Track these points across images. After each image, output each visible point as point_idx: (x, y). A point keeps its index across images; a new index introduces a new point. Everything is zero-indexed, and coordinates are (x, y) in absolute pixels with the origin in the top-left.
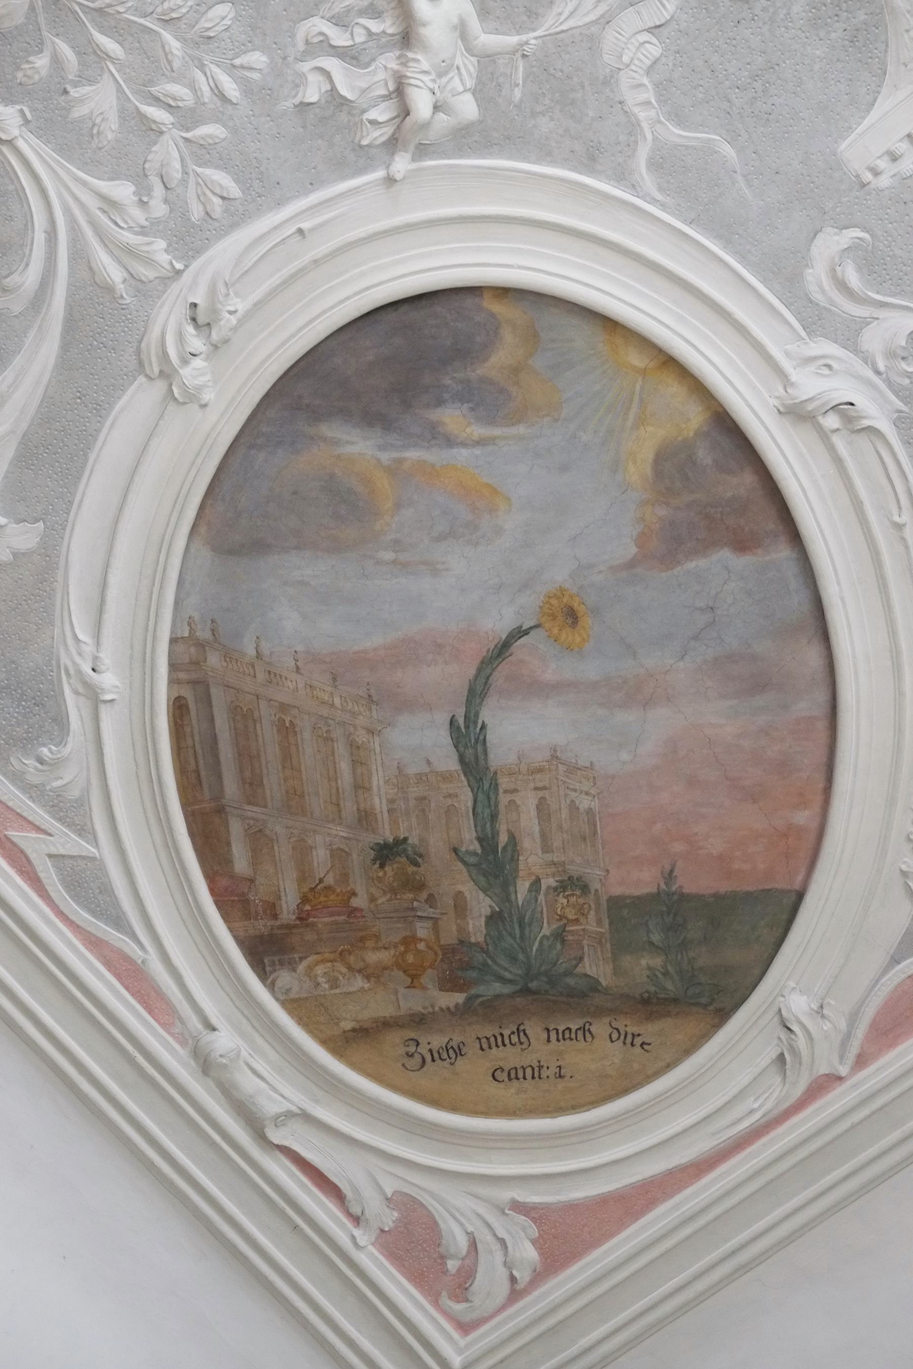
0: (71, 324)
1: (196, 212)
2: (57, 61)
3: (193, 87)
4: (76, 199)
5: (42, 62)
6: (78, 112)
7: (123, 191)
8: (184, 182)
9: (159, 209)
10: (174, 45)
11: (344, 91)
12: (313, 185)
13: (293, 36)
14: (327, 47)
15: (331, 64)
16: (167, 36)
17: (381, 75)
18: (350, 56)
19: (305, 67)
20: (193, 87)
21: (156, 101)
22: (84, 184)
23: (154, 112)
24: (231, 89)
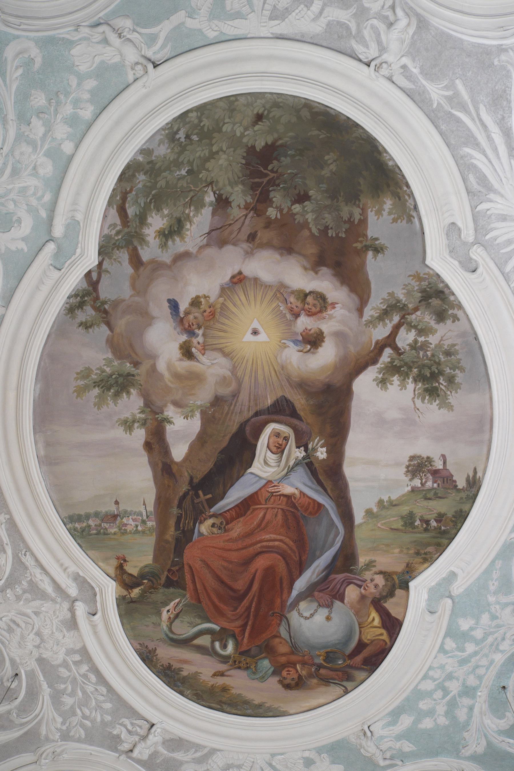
0: (26, 733)
1: (72, 734)
2: (66, 688)
3: (91, 713)
4: (48, 713)
5: (63, 686)
6: (62, 699)
7: (59, 720)
8: (74, 727)
9: (64, 728)
10: (94, 703)
11: (122, 737)
12: (102, 746)
13: (120, 719)
14: (125, 726)
15: (124, 730)
16: (94, 701)
17: (133, 739)
18: (130, 732)
19: (118, 726)
20: (91, 713)
21: (81, 710)
22: (52, 712)
23: (78, 711)
24: (99, 719)
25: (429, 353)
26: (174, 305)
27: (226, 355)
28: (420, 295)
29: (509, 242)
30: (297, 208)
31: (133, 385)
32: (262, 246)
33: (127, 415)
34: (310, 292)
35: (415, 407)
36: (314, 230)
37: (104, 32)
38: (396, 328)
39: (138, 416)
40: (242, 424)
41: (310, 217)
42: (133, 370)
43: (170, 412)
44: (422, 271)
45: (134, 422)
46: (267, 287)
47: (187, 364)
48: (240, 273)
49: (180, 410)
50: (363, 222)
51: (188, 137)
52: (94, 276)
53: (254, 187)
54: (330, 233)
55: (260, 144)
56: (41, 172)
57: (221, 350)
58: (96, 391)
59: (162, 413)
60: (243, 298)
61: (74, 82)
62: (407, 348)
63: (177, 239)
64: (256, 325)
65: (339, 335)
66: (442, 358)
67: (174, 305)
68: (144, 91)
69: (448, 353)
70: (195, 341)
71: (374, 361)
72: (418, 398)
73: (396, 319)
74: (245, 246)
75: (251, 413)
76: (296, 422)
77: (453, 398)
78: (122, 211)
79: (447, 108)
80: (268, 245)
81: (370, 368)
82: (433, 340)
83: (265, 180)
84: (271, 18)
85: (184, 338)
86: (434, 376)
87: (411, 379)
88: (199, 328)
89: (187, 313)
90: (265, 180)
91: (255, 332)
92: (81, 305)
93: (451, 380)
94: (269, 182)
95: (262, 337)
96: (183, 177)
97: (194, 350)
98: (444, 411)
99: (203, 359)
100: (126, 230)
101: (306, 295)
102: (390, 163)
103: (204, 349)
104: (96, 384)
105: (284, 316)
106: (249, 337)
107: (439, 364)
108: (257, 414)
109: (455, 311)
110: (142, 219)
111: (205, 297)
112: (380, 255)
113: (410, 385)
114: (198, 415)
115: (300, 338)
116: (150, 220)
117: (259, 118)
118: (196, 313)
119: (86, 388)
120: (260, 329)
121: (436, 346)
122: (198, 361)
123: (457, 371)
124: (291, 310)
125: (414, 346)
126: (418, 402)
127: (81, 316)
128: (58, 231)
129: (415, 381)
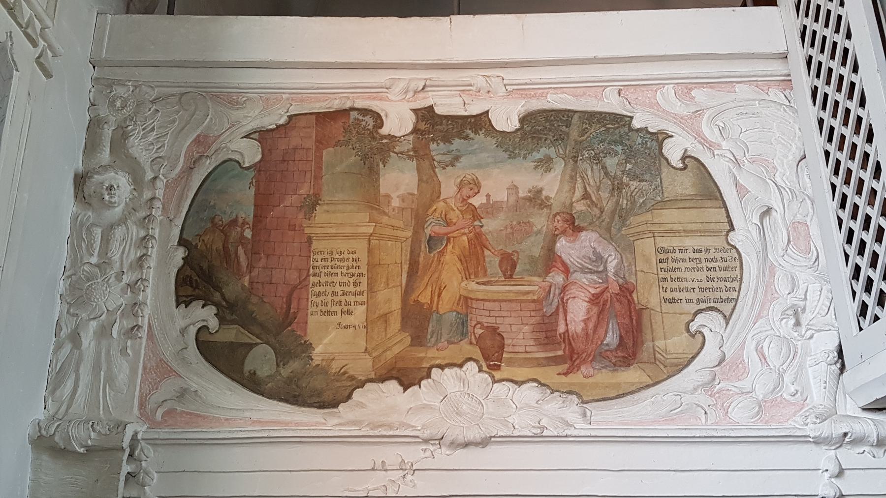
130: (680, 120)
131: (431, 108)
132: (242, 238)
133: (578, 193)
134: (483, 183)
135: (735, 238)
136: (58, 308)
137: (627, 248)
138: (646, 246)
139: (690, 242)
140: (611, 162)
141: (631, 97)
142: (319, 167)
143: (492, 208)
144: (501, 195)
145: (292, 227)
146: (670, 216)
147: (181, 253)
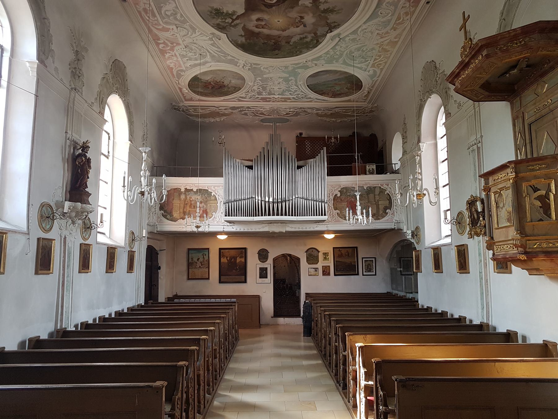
25: (220, 17)
26: (305, 26)
27: (288, 17)
28: (226, 28)
29: (202, 36)
30: (266, 42)
31: (322, 11)
32: (277, 36)
33: (325, 4)
34: (261, 28)
35: (222, 7)
36: (260, 38)
37: (316, 65)
38: (232, 22)
39: (322, 4)
40: (284, 2)
41: (262, 40)
42: (321, 14)
43: (310, 5)
44: (226, 32)
45: (324, 3)
46: (275, 29)
47: (302, 15)
48: (283, 32)
49: (306, 5)
50: (246, 40)
51: (297, 52)
52: (329, 31)
53: (279, 44)
54: (256, 38)
55: (277, 51)
56: (339, 47)
57: (290, 18)
58: (335, 10)
59: (313, 5)
60: (283, 28)
61: (326, 59)
62: (227, 18)
63: (302, 37)
64: (279, 23)
65: (252, 21)
66: (215, 17)
67: (305, 26)
68: (307, 58)
69: (214, 18)
70: (299, 20)
71: (238, 16)
72: (221, 9)
73: (233, 24)
74: (281, 36)
75: (280, 5)
76: (265, 3)
77: (210, 9)
78: (318, 41)
79: (227, 56)
80: (274, 36)
81: (240, 14)
82: (220, 20)
83: (275, 46)
84: (274, 66)
85: (302, 20)
86: (218, 13)
87: (225, 12)
88: (297, 22)
89: (301, 25)
90: (275, 46)
91: (279, 21)
92: (335, 26)
93: (211, 12)
94: (274, 45)
95: (276, 21)
96: (299, 46)
97: (300, 18)
98: (212, 6)
99: (296, 16)
100: (317, 38)
101: (262, 28)
102: (240, 48)
103: (296, 18)
104: (335, 11)
105: (269, 24)
106: (281, 20)
107: (216, 16)
108: (279, 5)
109: (214, 25)
110: (312, 40)
111: (295, 28)
112: (240, 34)
113: (225, 11)
114: (300, 5)
115: (264, 20)
116: (310, 40)
117: (277, 54)
118: (298, 25)
119: (339, 10)
120: (277, 22)
121: (218, 19)
122: (298, 16)
123: (210, 14)
124: (267, 25)
125: (226, 19)
126: (221, 8)
127: (336, 24)
128: (338, 39)
129: (223, 12)
130: (213, 191)
131: (186, 188)
132: (166, 203)
133: (202, 199)
134: (192, 197)
135: (218, 204)
136: (148, 211)
137: (207, 205)
138: (209, 205)
139: (213, 205)
140: (206, 195)
141: (209, 187)
142: (174, 195)
143: (193, 200)
144: (194, 199)
145: (171, 202)
146: (211, 202)
147: (160, 205)
